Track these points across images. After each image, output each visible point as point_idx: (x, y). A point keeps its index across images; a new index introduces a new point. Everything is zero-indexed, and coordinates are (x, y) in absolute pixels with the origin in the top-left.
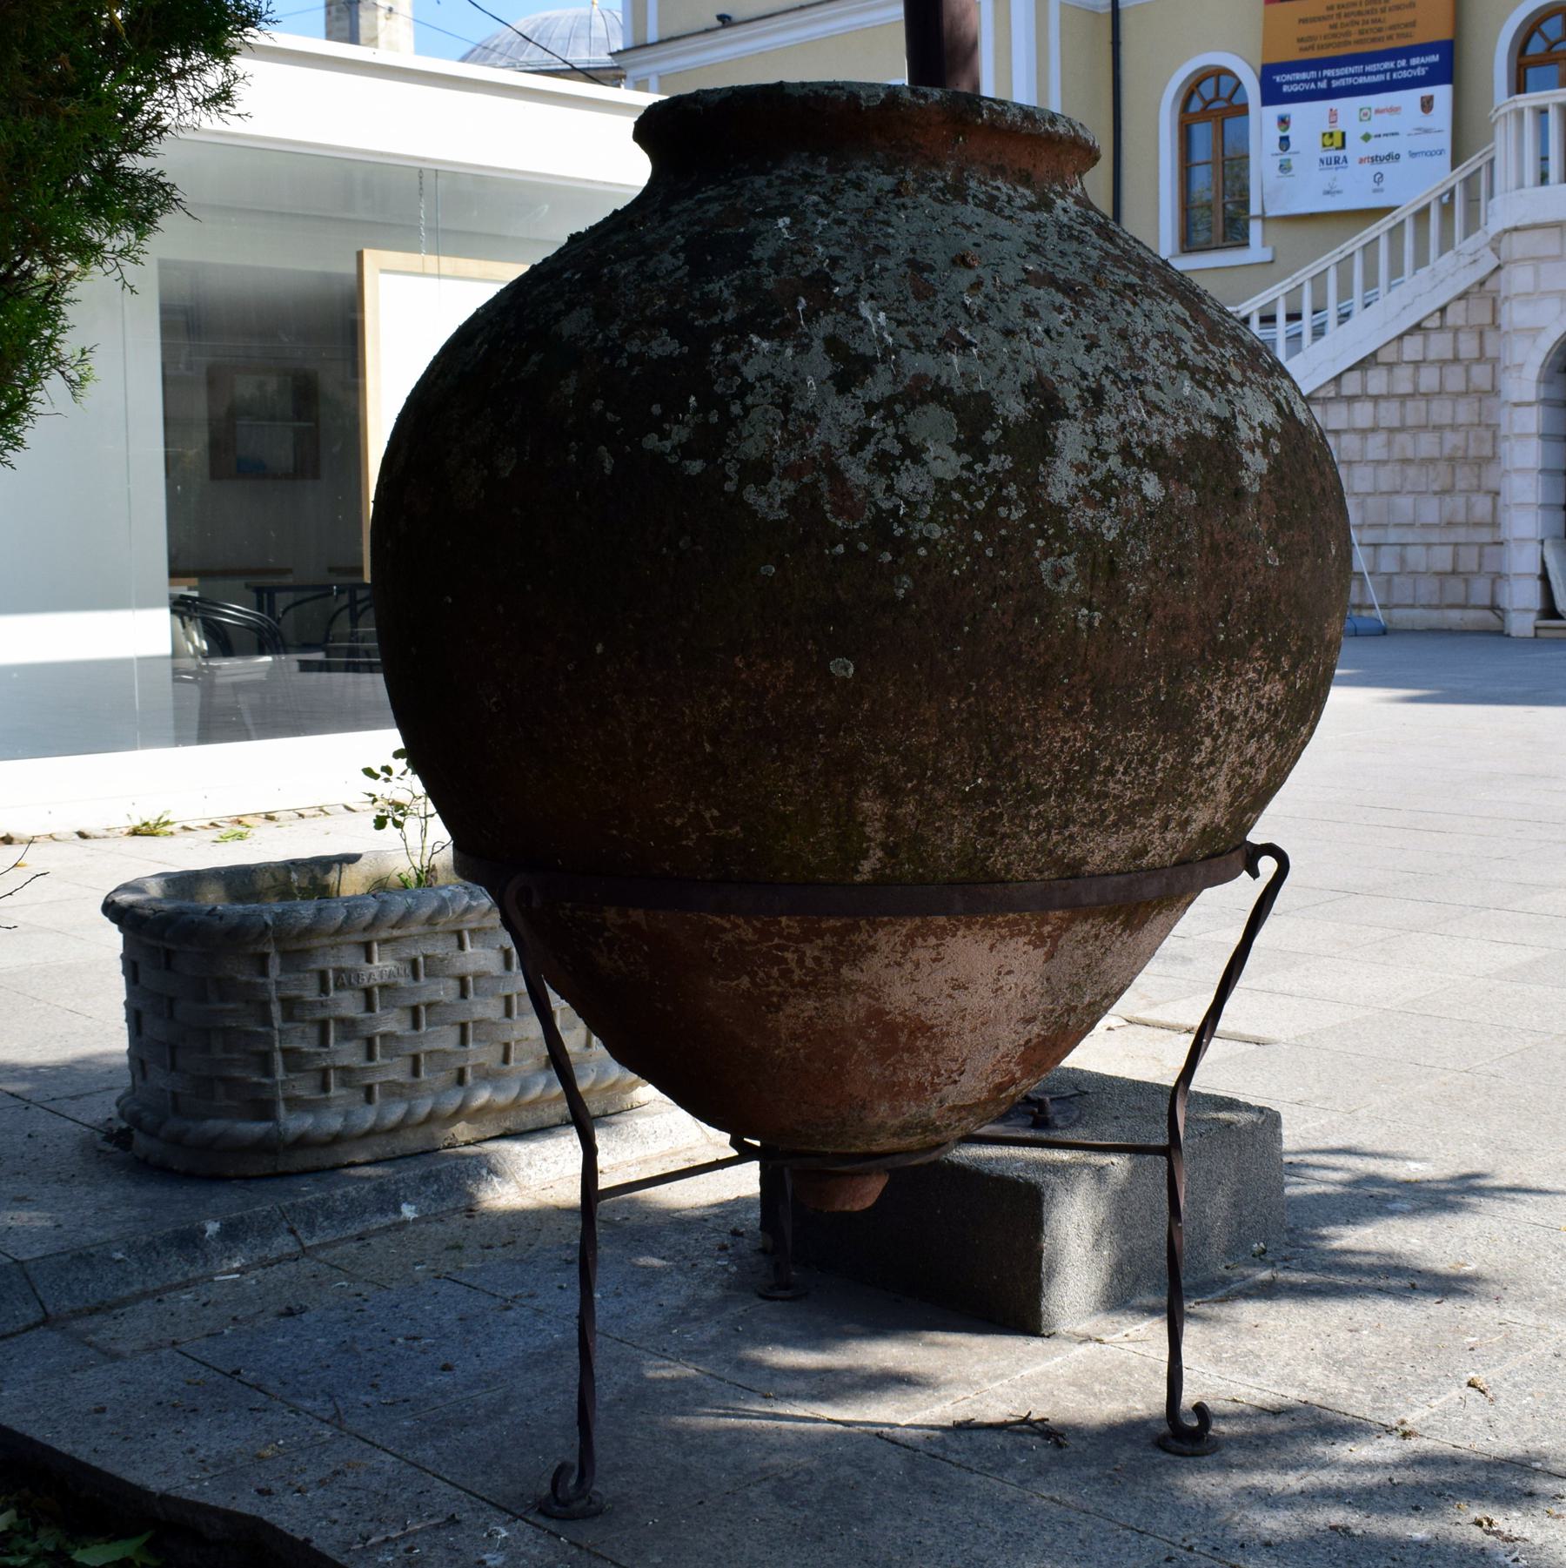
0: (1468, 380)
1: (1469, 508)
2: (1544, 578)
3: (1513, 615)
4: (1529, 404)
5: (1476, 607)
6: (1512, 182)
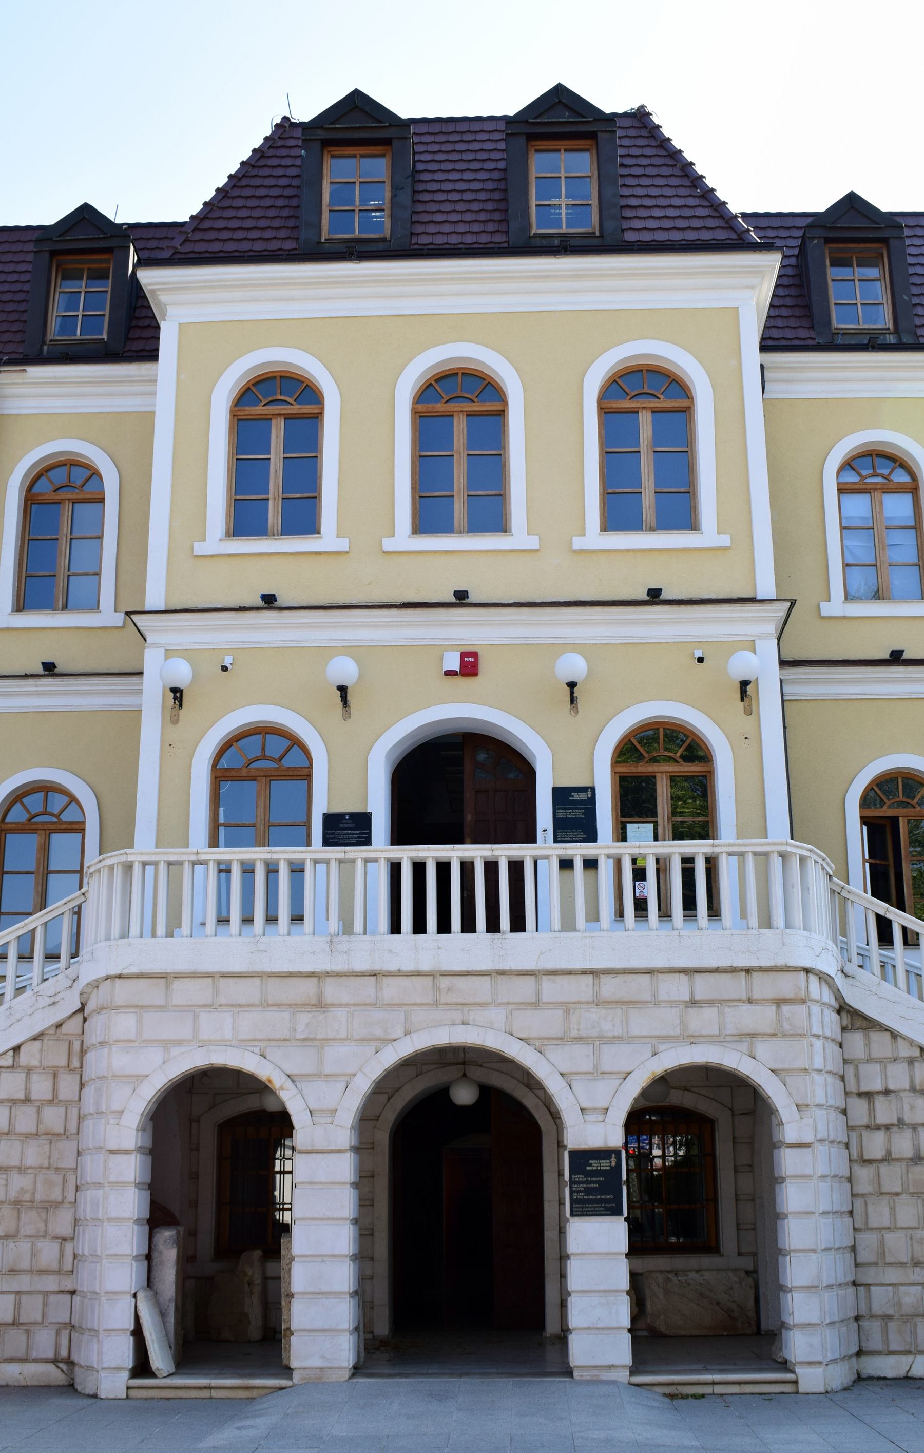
0: (39, 1121)
1: (34, 1254)
2: (138, 1333)
3: (103, 1374)
4: (127, 1152)
5: (36, 1361)
6: (102, 932)
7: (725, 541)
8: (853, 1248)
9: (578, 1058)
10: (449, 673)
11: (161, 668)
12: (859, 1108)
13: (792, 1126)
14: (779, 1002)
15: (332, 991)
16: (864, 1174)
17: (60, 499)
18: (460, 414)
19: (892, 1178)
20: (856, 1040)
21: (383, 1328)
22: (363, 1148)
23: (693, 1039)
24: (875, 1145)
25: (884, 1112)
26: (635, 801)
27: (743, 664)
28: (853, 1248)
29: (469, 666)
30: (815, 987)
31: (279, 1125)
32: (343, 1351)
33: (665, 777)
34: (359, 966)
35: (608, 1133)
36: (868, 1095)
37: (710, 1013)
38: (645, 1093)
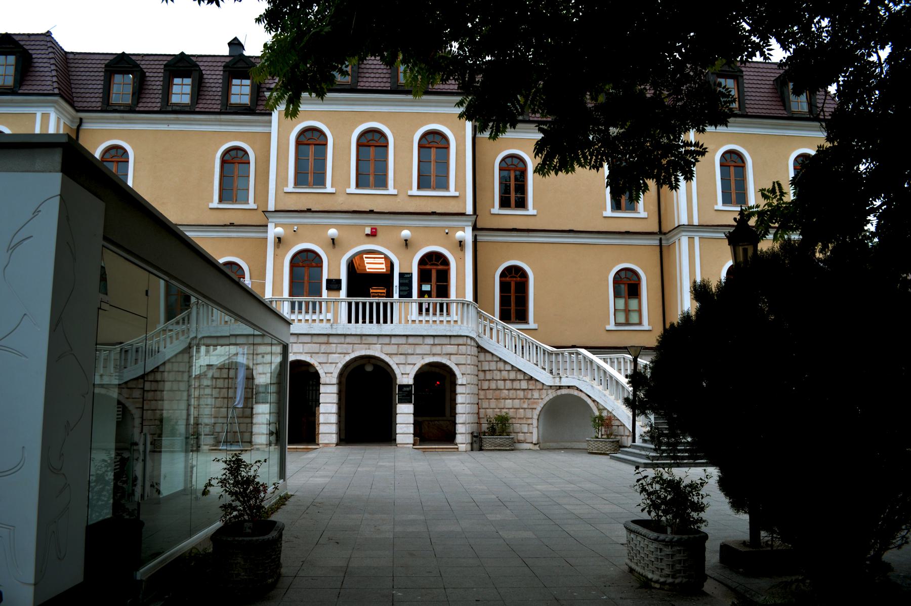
7: (457, 194)
8: (478, 413)
9: (401, 359)
10: (367, 235)
11: (274, 231)
12: (481, 375)
13: (460, 380)
14: (458, 345)
15: (332, 340)
16: (482, 393)
17: (234, 159)
18: (372, 142)
19: (490, 394)
20: (482, 356)
21: (343, 437)
22: (340, 384)
23: (434, 355)
24: (486, 385)
25: (489, 376)
26: (424, 277)
27: (459, 234)
28: (478, 413)
29: (373, 234)
30: (469, 341)
31: (317, 375)
32: (334, 439)
33: (435, 270)
34: (339, 332)
35: (409, 380)
36: (484, 371)
37: (439, 347)
38: (420, 369)
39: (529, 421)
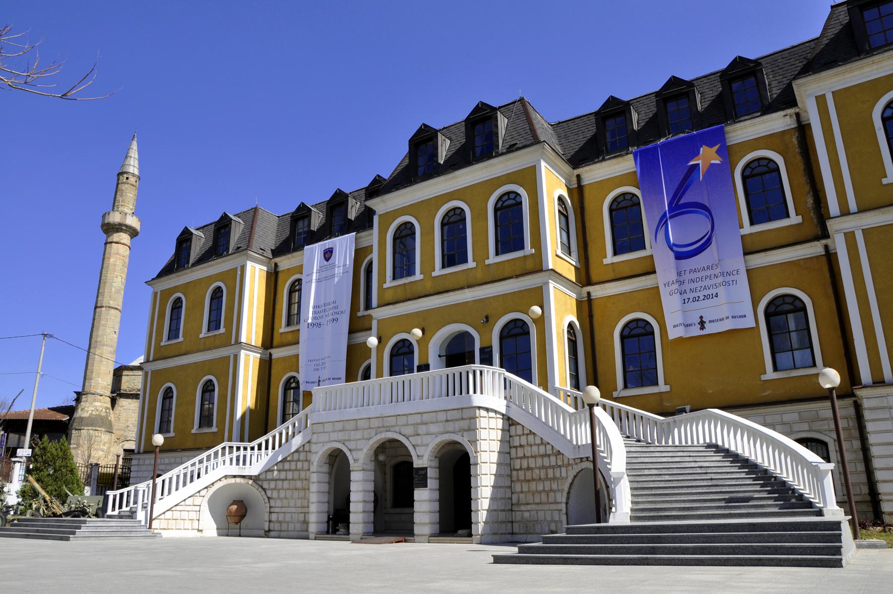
16: (514, 473)
36: (516, 447)
39: (559, 507)
